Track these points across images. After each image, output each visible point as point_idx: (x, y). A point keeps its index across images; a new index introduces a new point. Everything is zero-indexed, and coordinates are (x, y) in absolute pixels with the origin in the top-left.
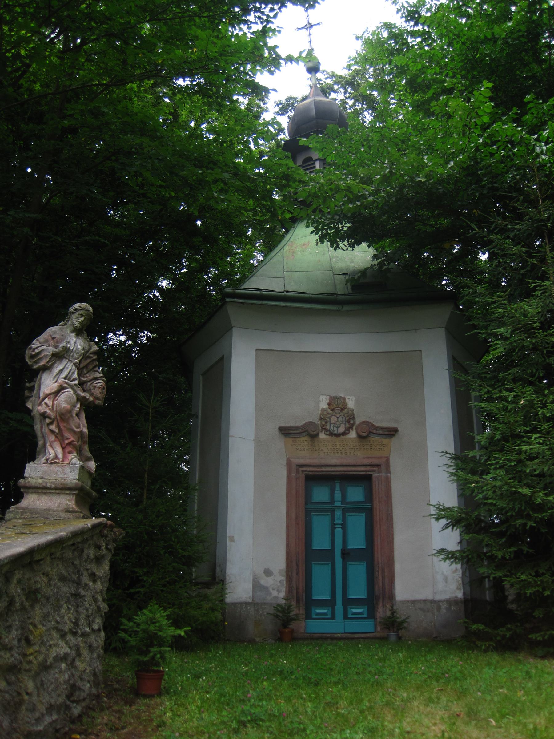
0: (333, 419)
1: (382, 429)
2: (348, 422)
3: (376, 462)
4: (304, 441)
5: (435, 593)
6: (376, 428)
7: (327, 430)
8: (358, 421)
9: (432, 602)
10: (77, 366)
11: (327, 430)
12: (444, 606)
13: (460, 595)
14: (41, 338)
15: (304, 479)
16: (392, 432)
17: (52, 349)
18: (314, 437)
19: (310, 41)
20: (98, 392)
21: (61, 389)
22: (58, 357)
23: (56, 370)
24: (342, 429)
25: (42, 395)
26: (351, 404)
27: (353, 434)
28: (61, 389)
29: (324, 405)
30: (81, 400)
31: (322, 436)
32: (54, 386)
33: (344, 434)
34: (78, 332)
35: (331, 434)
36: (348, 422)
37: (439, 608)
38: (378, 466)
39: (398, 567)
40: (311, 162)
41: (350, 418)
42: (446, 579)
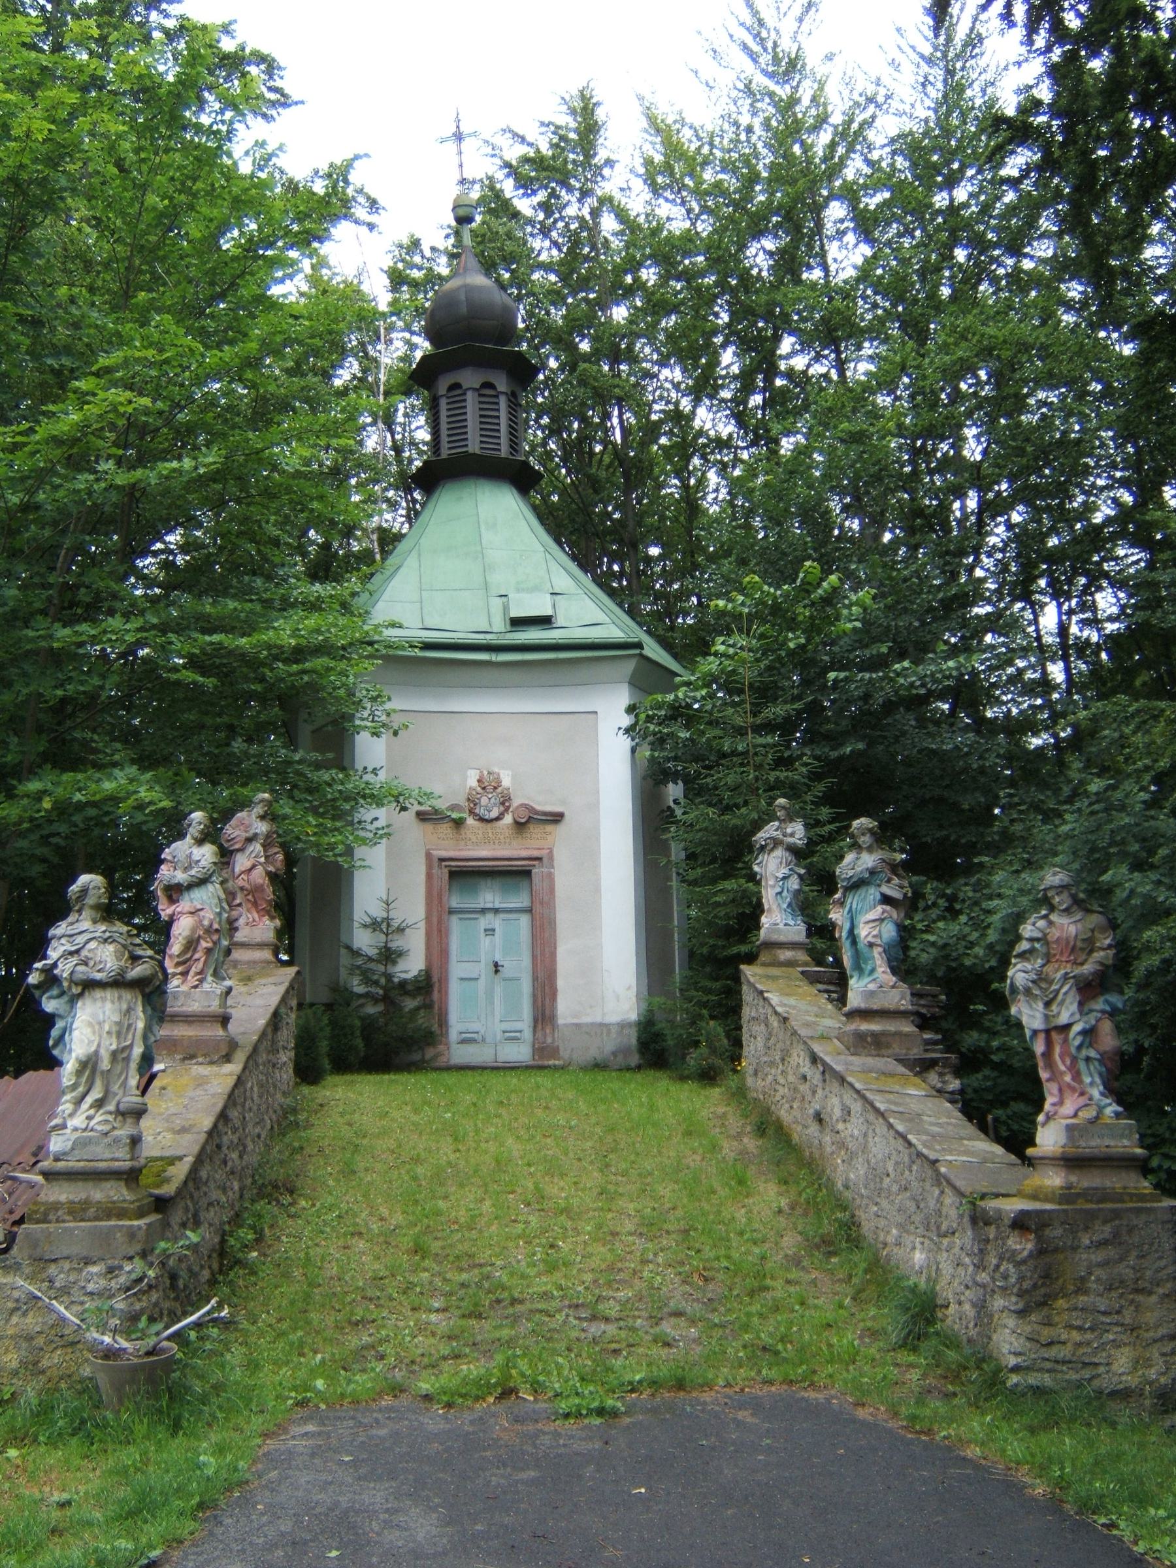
0: (484, 801)
1: (545, 814)
2: (503, 803)
3: (536, 853)
4: (445, 829)
5: (604, 1015)
6: (537, 812)
7: (475, 815)
8: (516, 803)
9: (601, 1025)
10: (264, 846)
11: (475, 815)
12: (614, 1030)
13: (633, 1016)
14: (233, 822)
15: (446, 876)
16: (556, 818)
17: (245, 835)
18: (458, 823)
19: (461, 166)
20: (279, 865)
21: (254, 867)
22: (249, 840)
23: (247, 852)
24: (494, 813)
25: (237, 870)
26: (506, 782)
27: (508, 819)
28: (254, 867)
29: (472, 782)
30: (269, 874)
31: (470, 821)
32: (248, 864)
33: (498, 819)
34: (262, 818)
35: (482, 819)
36: (503, 803)
37: (609, 1032)
38: (539, 859)
39: (561, 983)
40: (459, 392)
41: (505, 801)
42: (618, 998)
